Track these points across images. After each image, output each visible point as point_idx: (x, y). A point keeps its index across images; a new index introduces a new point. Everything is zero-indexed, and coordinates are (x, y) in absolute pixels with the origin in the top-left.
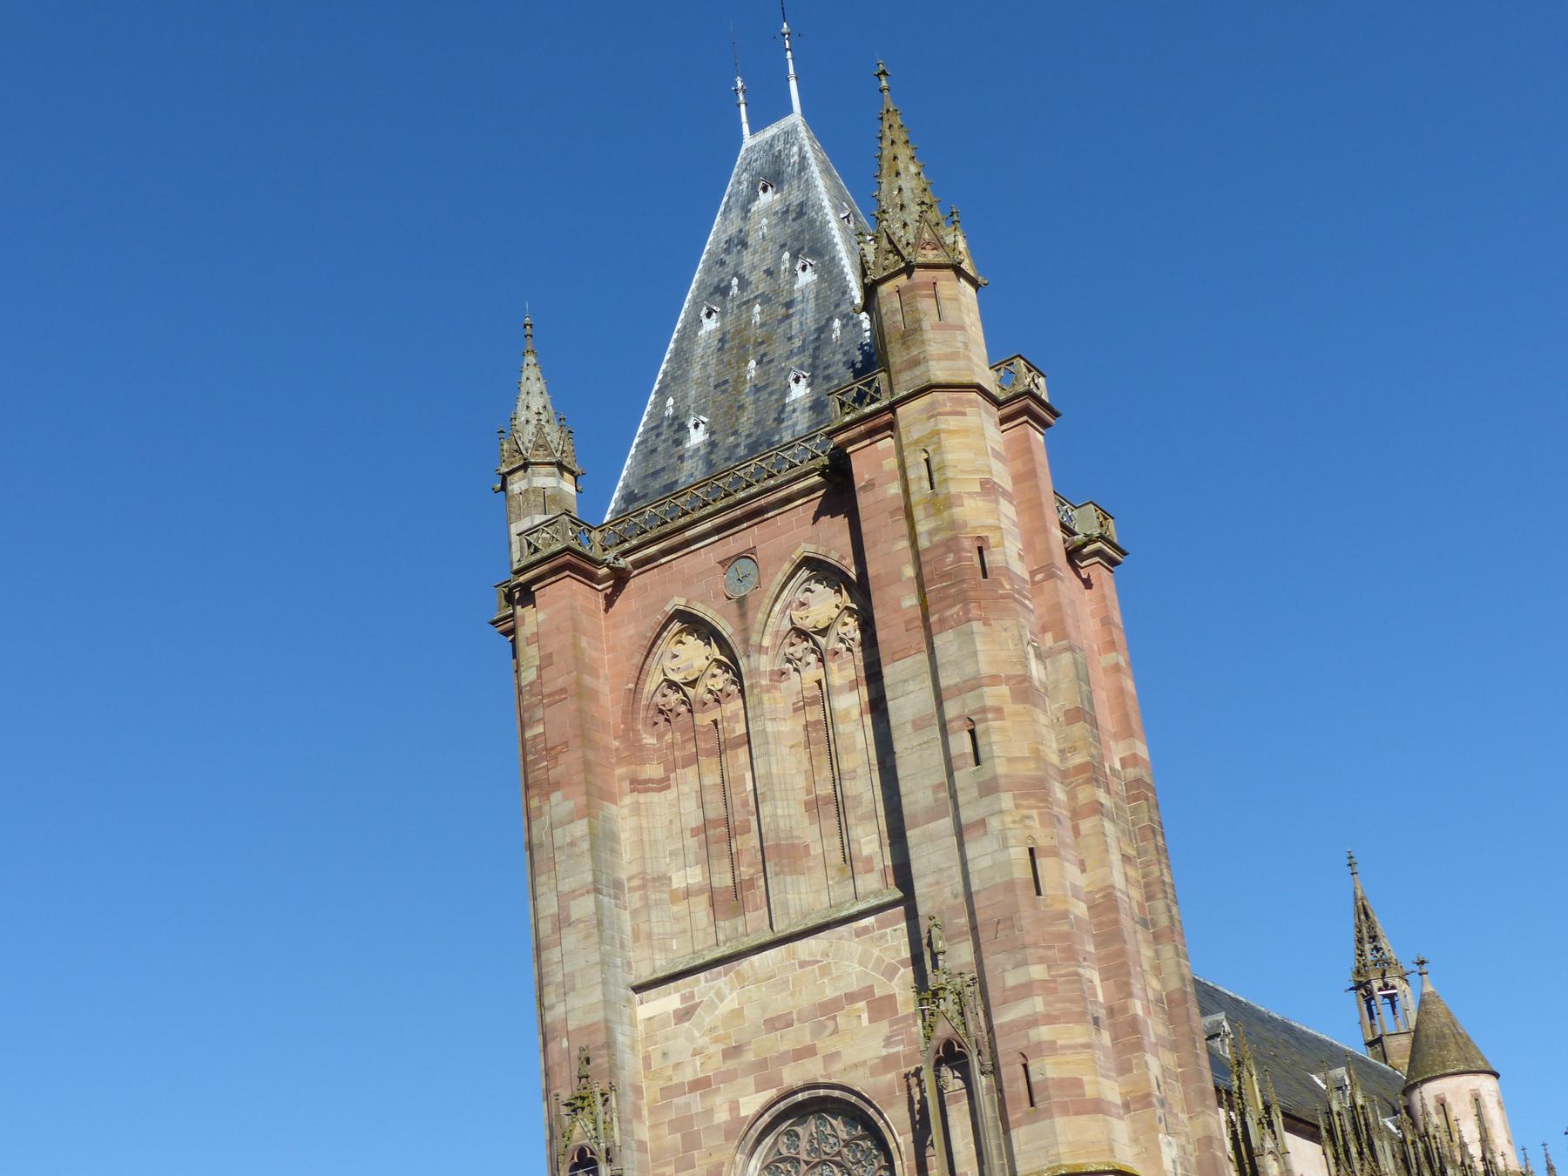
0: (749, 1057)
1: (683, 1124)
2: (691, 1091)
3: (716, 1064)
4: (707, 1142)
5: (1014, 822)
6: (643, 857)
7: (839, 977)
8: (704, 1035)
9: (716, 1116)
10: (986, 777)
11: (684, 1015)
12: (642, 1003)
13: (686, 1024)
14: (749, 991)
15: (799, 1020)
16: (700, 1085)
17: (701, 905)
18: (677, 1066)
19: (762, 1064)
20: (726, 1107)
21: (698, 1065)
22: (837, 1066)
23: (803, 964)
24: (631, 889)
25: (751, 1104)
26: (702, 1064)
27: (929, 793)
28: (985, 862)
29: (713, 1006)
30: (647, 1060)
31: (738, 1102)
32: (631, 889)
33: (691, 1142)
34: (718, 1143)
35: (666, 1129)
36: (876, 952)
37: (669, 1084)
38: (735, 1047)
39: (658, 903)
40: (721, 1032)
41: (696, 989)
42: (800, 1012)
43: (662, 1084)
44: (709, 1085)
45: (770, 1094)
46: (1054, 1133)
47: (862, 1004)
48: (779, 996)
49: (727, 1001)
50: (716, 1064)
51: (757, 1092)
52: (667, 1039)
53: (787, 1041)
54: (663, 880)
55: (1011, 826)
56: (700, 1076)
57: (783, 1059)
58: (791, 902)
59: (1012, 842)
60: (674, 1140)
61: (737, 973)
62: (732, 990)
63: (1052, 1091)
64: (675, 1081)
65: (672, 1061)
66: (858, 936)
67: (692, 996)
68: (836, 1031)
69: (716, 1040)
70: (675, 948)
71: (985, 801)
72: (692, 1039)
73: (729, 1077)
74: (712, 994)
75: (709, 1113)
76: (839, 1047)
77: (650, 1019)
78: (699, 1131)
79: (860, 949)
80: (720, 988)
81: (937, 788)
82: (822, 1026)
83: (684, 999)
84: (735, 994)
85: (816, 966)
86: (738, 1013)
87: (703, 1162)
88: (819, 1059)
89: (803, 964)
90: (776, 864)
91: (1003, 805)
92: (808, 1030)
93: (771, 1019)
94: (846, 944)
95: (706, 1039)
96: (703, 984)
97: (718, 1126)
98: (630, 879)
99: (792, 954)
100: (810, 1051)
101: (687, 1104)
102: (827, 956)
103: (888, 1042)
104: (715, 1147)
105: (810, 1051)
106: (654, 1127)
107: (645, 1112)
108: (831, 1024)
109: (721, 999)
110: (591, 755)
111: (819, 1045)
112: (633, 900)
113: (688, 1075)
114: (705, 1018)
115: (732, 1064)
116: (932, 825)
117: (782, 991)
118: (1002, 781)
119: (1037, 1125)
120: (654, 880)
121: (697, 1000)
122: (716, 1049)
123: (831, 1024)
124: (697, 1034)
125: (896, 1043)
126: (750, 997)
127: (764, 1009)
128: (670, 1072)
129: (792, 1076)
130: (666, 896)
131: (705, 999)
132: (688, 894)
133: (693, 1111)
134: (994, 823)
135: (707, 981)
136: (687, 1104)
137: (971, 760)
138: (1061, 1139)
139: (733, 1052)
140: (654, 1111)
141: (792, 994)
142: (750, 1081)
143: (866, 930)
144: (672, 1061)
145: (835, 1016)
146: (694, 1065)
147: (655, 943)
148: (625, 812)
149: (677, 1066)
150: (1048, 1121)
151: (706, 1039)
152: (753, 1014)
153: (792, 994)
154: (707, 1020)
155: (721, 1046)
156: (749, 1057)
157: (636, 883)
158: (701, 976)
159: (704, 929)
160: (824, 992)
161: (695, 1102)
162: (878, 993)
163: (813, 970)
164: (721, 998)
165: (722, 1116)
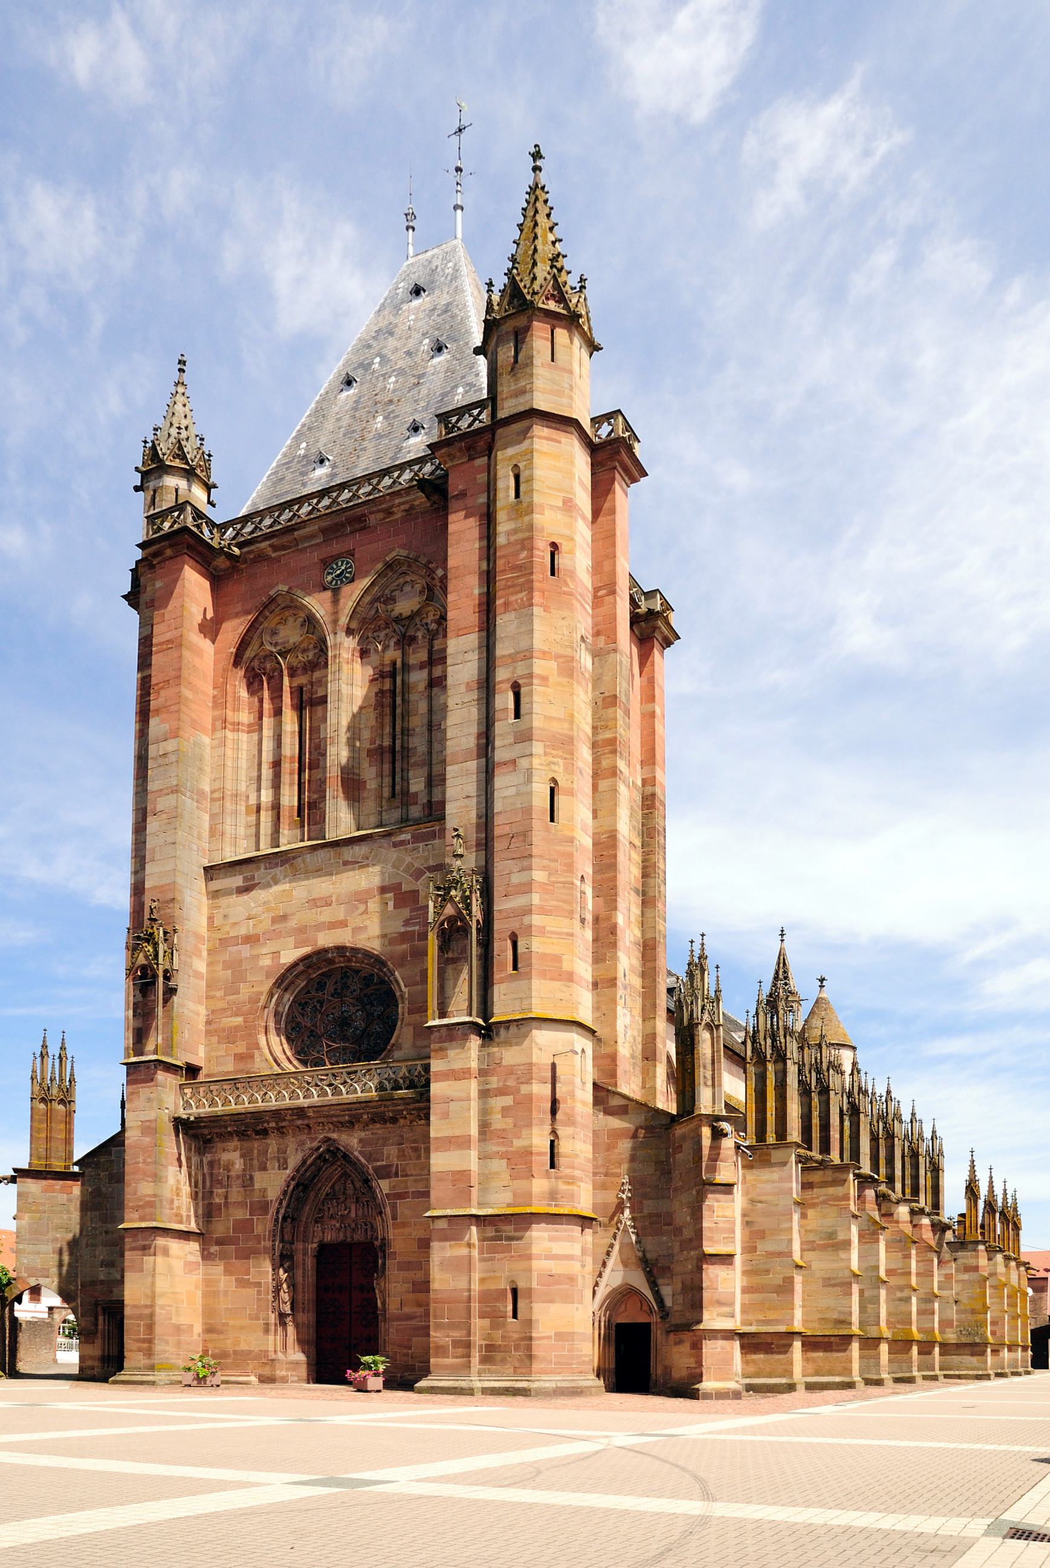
0: (293, 923)
3: (266, 924)
16: (250, 940)
19: (302, 930)
22: (363, 936)
25: (290, 955)
28: (512, 791)
36: (408, 859)
52: (229, 906)
53: (326, 915)
57: (320, 927)
65: (231, 920)
67: (253, 878)
68: (366, 912)
69: (268, 910)
73: (274, 935)
76: (367, 923)
93: (314, 899)
100: (343, 924)
103: (407, 923)
105: (343, 924)
113: (243, 931)
125: (414, 924)
129: (326, 940)
133: (243, 955)
156: (293, 923)
160: (360, 885)
161: (245, 951)
162: (404, 888)
165: (266, 962)
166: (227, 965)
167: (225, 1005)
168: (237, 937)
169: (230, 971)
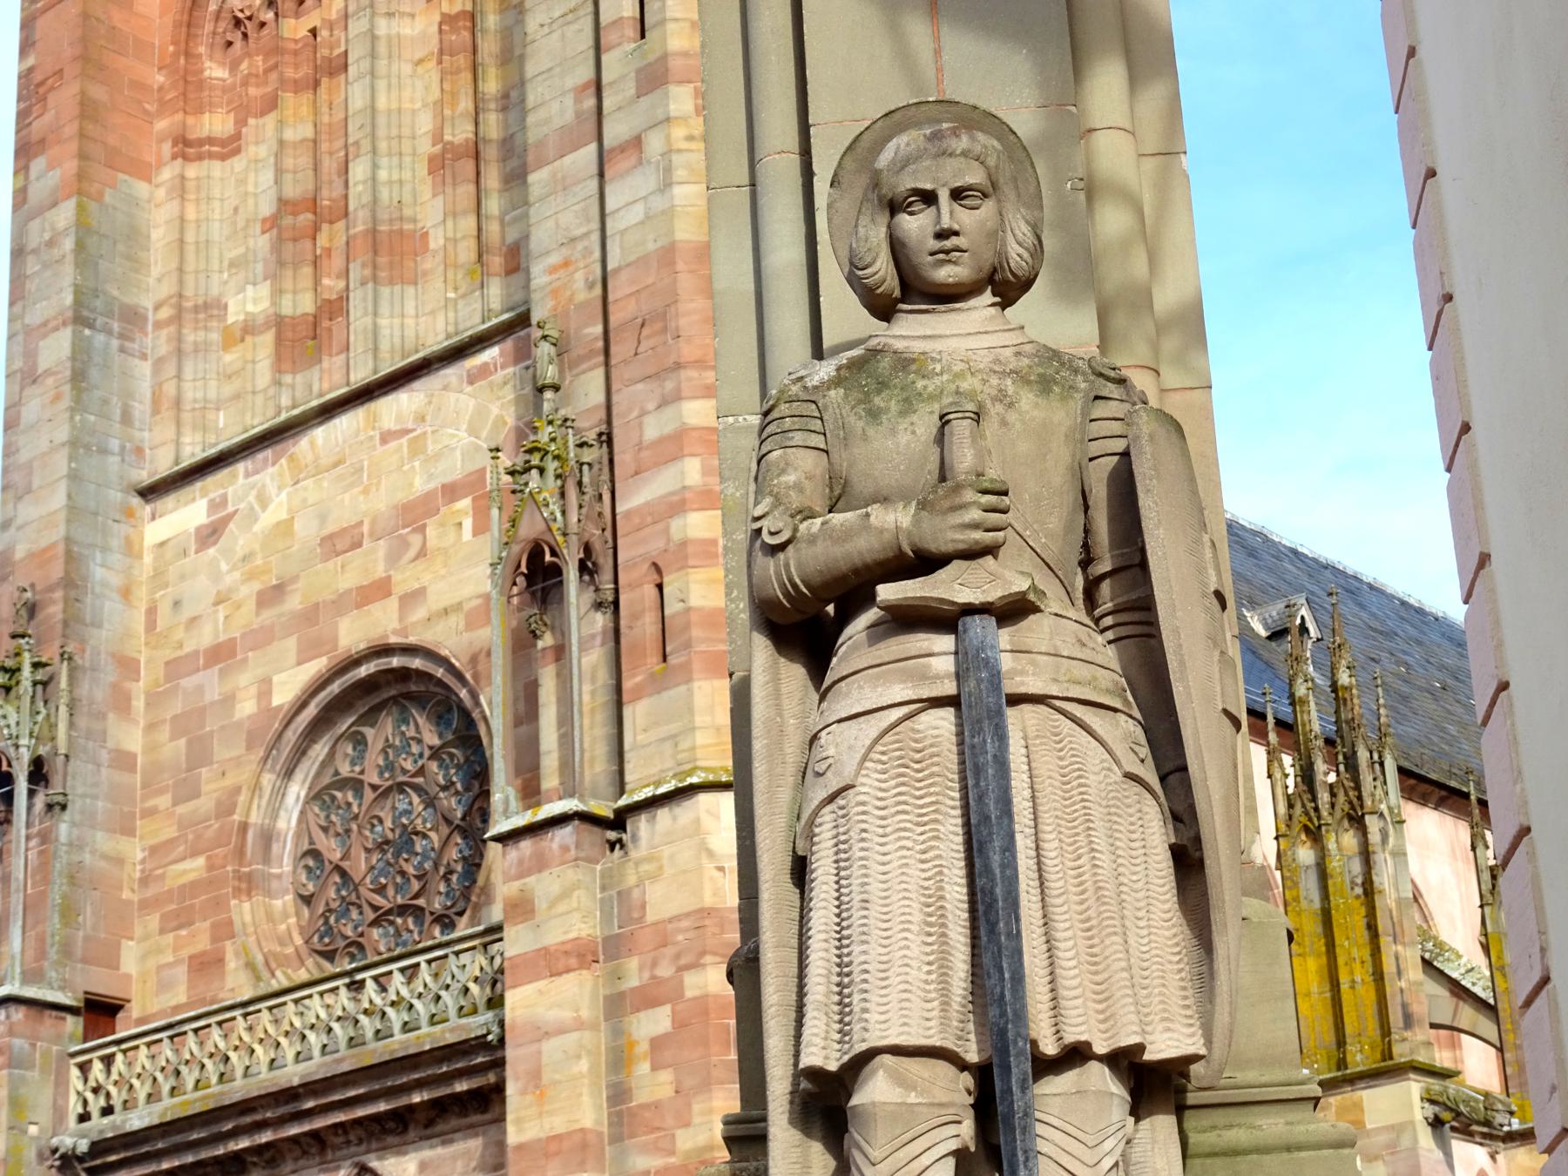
1: (191, 726)
2: (207, 666)
4: (221, 753)
5: (690, 138)
6: (181, 270)
7: (437, 456)
8: (233, 568)
9: (238, 706)
10: (651, 58)
11: (210, 534)
12: (153, 518)
13: (212, 551)
14: (305, 489)
15: (371, 534)
16: (222, 654)
17: (265, 343)
18: (193, 621)
19: (311, 615)
20: (253, 690)
21: (221, 619)
23: (386, 437)
24: (158, 325)
25: (289, 684)
26: (226, 617)
27: (569, 101)
29: (252, 517)
30: (152, 612)
31: (270, 681)
32: (158, 325)
33: (199, 755)
34: (234, 753)
35: (164, 734)
37: (179, 653)
38: (275, 587)
39: (201, 349)
40: (259, 562)
41: (230, 490)
42: (373, 523)
43: (169, 654)
44: (233, 654)
45: (317, 666)
46: (691, 710)
47: (465, 503)
48: (347, 497)
49: (272, 507)
50: (247, 616)
51: (299, 663)
52: (183, 577)
53: (351, 573)
54: (212, 308)
55: (684, 145)
56: (222, 638)
58: (385, 332)
59: (680, 174)
60: (174, 749)
61: (292, 459)
62: (280, 488)
63: (696, 633)
64: (187, 649)
65: (187, 613)
66: (471, 383)
67: (224, 501)
69: (250, 577)
70: (221, 425)
71: (645, 102)
72: (216, 577)
73: (261, 638)
74: (251, 498)
75: (229, 700)
77: (162, 544)
78: (212, 732)
79: (472, 403)
80: (264, 486)
81: (579, 91)
82: (404, 544)
83: (214, 506)
84: (283, 496)
85: (404, 441)
86: (284, 528)
87: (213, 786)
88: (392, 603)
89: (386, 437)
90: (364, 265)
91: (672, 107)
92: (381, 553)
94: (453, 396)
95: (237, 575)
96: (241, 480)
97: (239, 724)
98: (157, 308)
99: (373, 420)
100: (379, 590)
101: (200, 689)
102: (423, 419)
104: (230, 759)
105: (379, 590)
106: (151, 727)
107: (139, 704)
108: (416, 541)
109: (264, 507)
110: (98, 92)
111: (397, 577)
112: (157, 342)
113: (205, 637)
114: (239, 539)
115: (268, 615)
116: (568, 160)
117: (352, 485)
118: (675, 64)
119: (666, 695)
120: (196, 309)
121: (230, 509)
122: (248, 591)
123: (416, 541)
124: (224, 567)
126: (305, 500)
127: (323, 518)
128: (179, 634)
130: (215, 336)
131: (242, 506)
132: (249, 329)
133: (208, 698)
134: (654, 144)
135: (247, 475)
136: (200, 689)
137: (631, 31)
138: (699, 720)
139: (274, 594)
140: (153, 700)
141: (366, 492)
142: (291, 643)
143: (484, 371)
144: (187, 613)
145: (424, 526)
146: (216, 622)
147: (186, 417)
148: (161, 193)
149: (193, 621)
150: (682, 688)
151: (237, 575)
152: (307, 530)
153: (366, 492)
154: (241, 542)
155: (256, 586)
157: (165, 313)
158: (241, 467)
159: (265, 390)
161: (210, 684)
163: (401, 446)
164: (264, 502)
165: (247, 707)
166: (180, 726)
167: (170, 832)
168: (196, 652)
169: (182, 742)
